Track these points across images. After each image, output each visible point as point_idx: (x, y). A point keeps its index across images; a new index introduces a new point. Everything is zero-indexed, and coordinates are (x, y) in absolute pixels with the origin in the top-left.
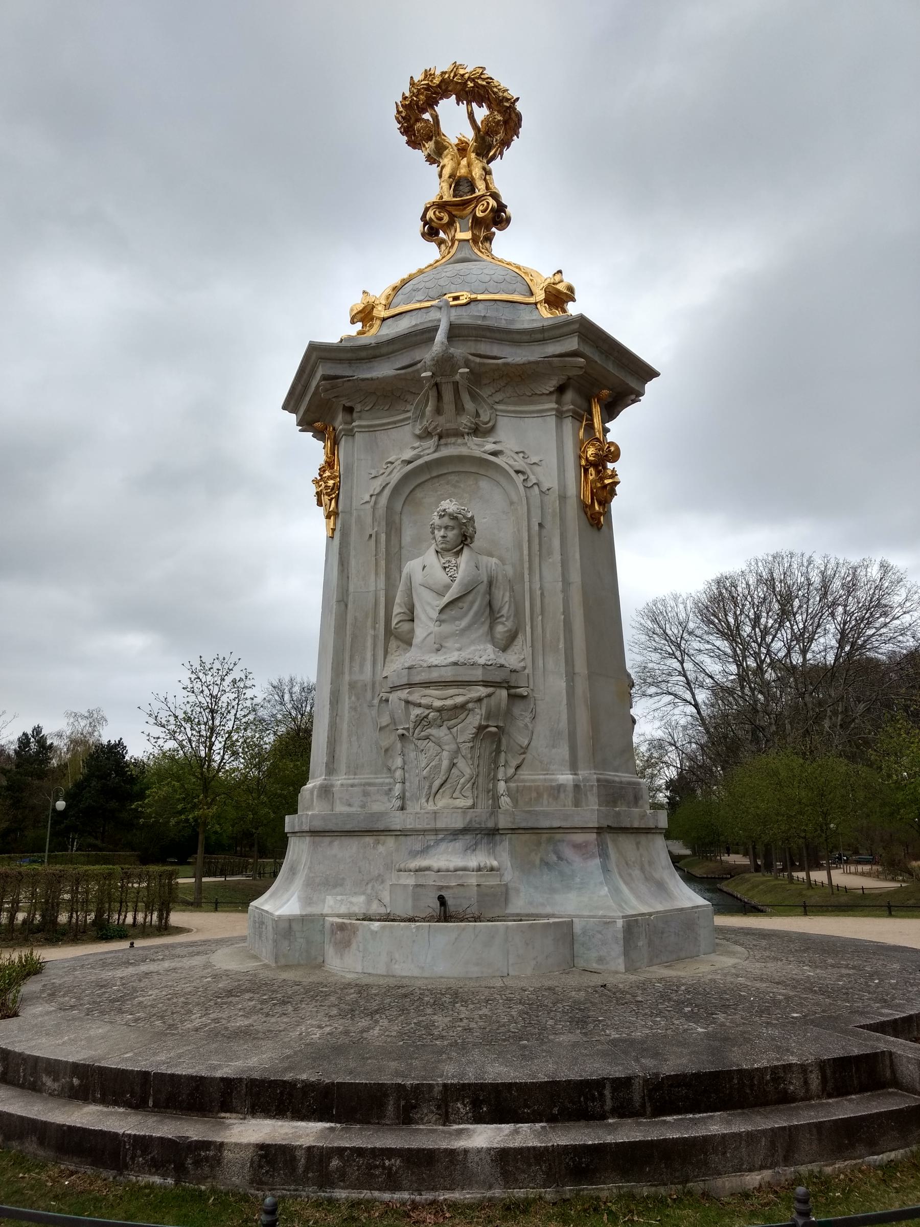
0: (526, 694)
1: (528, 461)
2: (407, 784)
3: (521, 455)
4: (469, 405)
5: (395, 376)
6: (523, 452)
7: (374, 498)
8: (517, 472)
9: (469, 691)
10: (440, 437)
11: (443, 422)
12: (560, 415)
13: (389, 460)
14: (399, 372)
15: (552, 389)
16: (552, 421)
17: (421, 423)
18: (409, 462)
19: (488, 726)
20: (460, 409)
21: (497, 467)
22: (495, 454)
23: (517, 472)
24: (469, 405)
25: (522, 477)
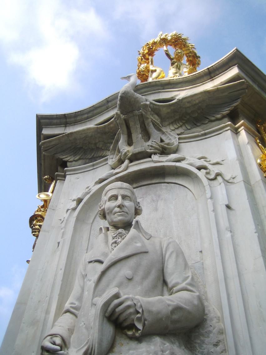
1: (211, 163)
5: (96, 127)
7: (69, 211)
8: (199, 168)
20: (147, 136)
23: (199, 168)
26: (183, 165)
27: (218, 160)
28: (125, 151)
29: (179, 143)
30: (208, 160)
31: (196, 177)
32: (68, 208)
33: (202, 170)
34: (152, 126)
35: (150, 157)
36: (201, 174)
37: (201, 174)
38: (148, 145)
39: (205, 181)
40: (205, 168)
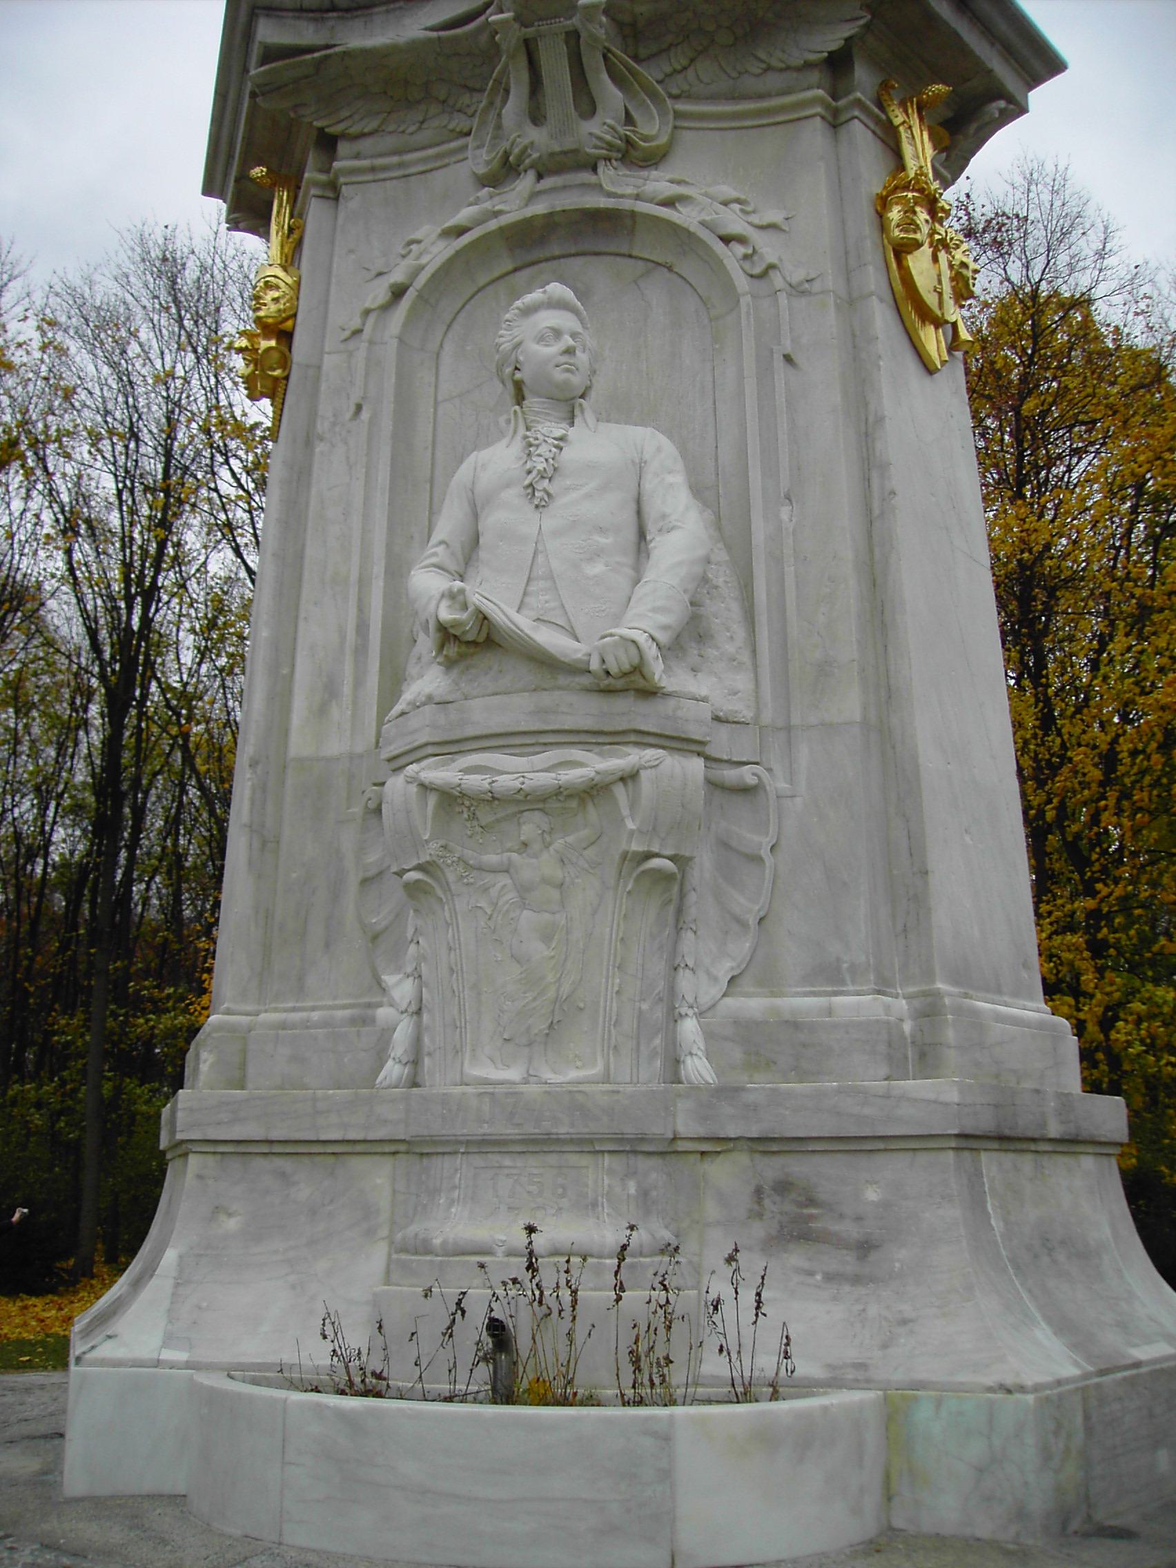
0: (751, 780)
2: (425, 1017)
3: (736, 207)
4: (611, 95)
5: (430, 40)
6: (738, 201)
8: (726, 240)
9: (600, 754)
10: (540, 177)
11: (539, 139)
12: (835, 122)
13: (413, 237)
14: (442, 33)
15: (812, 57)
16: (814, 134)
17: (493, 146)
18: (460, 231)
19: (649, 856)
20: (587, 105)
21: (675, 230)
22: (669, 203)
23: (726, 240)
24: (611, 95)
25: (740, 250)
26: (684, 216)
27: (773, 215)
28: (526, 141)
29: (675, 127)
30: (749, 209)
31: (715, 266)
32: (368, 304)
33: (733, 245)
34: (605, 76)
35: (595, 169)
36: (730, 256)
37: (730, 256)
38: (591, 134)
39: (741, 282)
40: (741, 240)
